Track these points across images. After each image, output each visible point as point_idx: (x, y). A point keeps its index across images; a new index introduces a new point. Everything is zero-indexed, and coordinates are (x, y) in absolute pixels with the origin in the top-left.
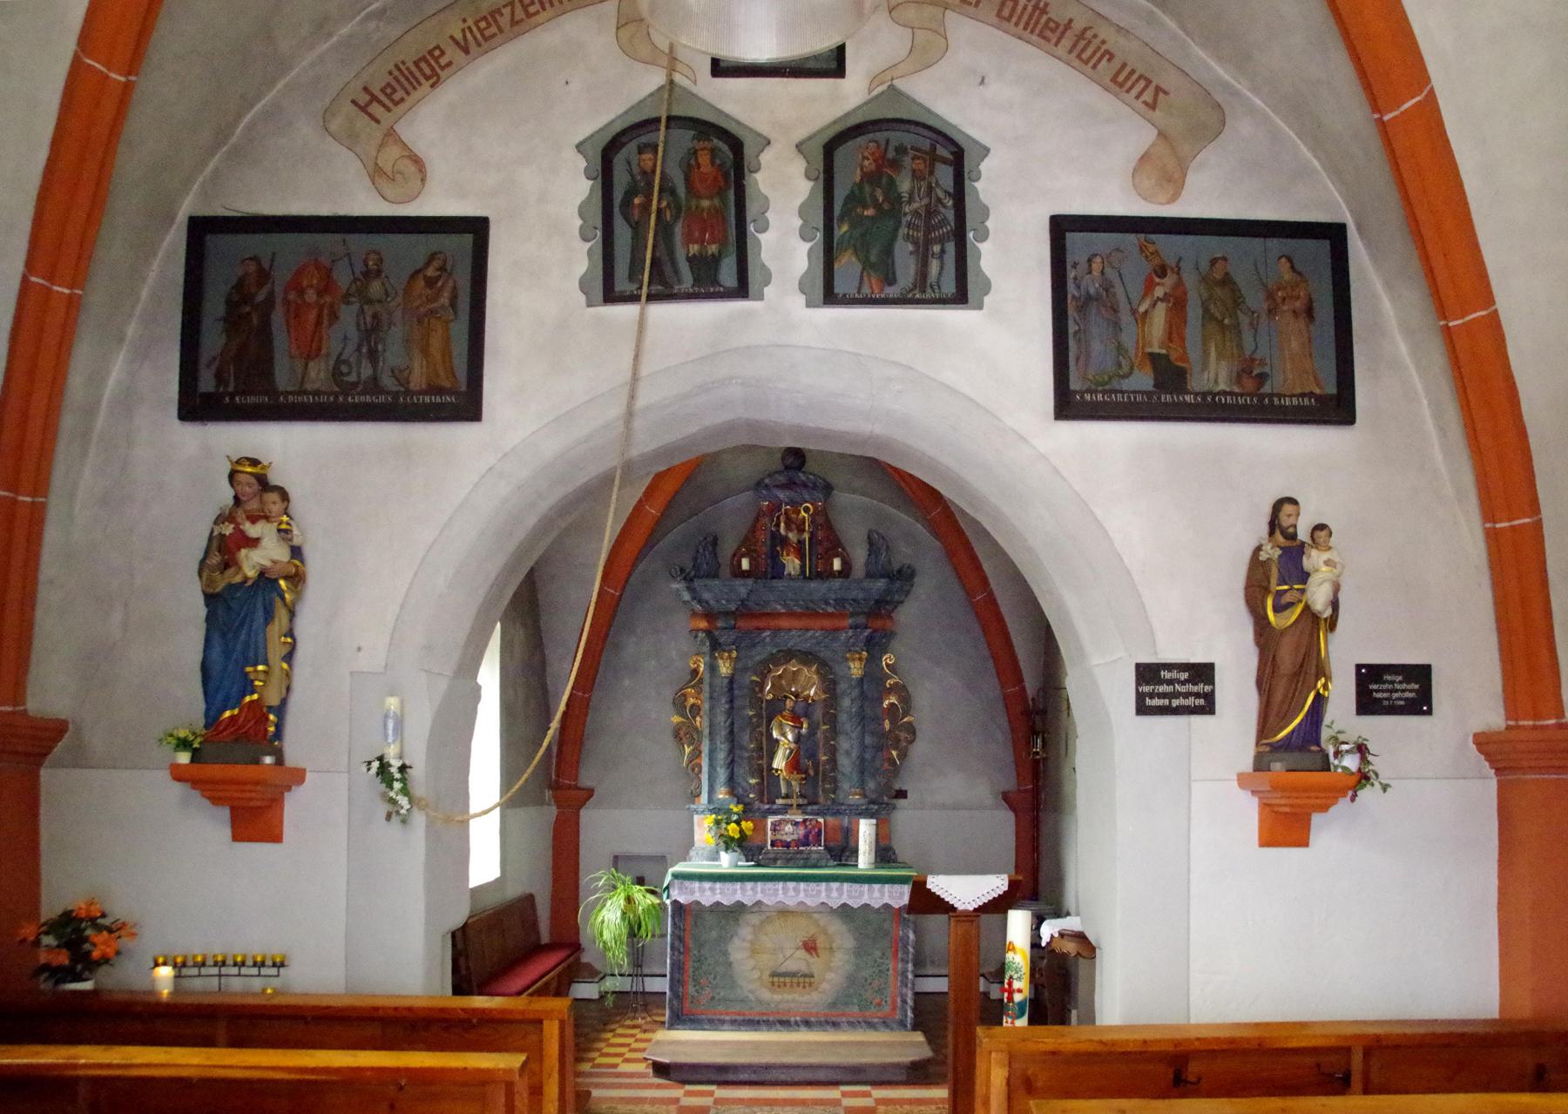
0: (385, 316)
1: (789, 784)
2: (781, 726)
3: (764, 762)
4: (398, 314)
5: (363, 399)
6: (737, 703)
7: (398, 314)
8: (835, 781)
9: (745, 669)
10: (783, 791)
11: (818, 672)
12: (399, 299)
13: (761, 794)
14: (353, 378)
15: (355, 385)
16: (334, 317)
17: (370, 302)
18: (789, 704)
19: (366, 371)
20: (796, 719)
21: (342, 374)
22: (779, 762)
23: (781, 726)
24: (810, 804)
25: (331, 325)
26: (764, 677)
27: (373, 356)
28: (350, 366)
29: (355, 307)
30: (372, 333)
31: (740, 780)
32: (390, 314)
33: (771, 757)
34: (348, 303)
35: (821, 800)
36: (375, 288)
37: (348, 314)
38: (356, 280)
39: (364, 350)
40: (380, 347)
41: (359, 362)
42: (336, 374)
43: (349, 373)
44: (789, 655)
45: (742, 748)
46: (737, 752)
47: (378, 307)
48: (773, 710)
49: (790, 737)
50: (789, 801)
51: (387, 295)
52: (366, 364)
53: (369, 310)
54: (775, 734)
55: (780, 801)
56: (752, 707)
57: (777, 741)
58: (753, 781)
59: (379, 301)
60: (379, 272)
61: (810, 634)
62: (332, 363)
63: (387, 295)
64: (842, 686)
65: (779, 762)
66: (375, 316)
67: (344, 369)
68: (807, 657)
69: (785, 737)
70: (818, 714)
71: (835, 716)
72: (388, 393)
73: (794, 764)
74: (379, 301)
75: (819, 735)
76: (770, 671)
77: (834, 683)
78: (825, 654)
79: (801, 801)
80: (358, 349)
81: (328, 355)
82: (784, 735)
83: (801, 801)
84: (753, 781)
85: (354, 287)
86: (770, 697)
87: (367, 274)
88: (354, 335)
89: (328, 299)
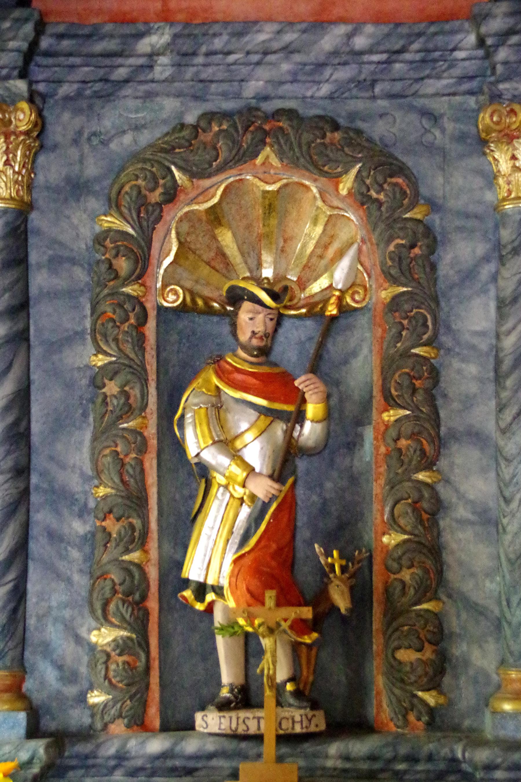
1: (250, 649)
2: (217, 408)
3: (150, 558)
6: (43, 318)
8: (437, 635)
9: (76, 188)
10: (228, 675)
11: (362, 198)
13: (135, 685)
18: (251, 322)
20: (278, 387)
22: (212, 555)
23: (217, 408)
24: (336, 729)
26: (148, 216)
31: (54, 633)
33: (181, 528)
35: (382, 705)
44: (251, 129)
45: (60, 497)
46: (41, 517)
48: (176, 351)
49: (256, 452)
50: (248, 721)
54: (196, 442)
55: (210, 721)
56: (99, 336)
57: (204, 471)
58: (104, 637)
61: (330, 40)
64: (461, 251)
65: (212, 555)
68: (318, 139)
69: (235, 455)
70: (364, 363)
71: (435, 374)
73: (275, 563)
75: (371, 446)
76: (172, 194)
77: (429, 239)
78: (390, 126)
79: (298, 718)
82: (227, 444)
83: (298, 718)
84: (104, 637)
86: (172, 300)
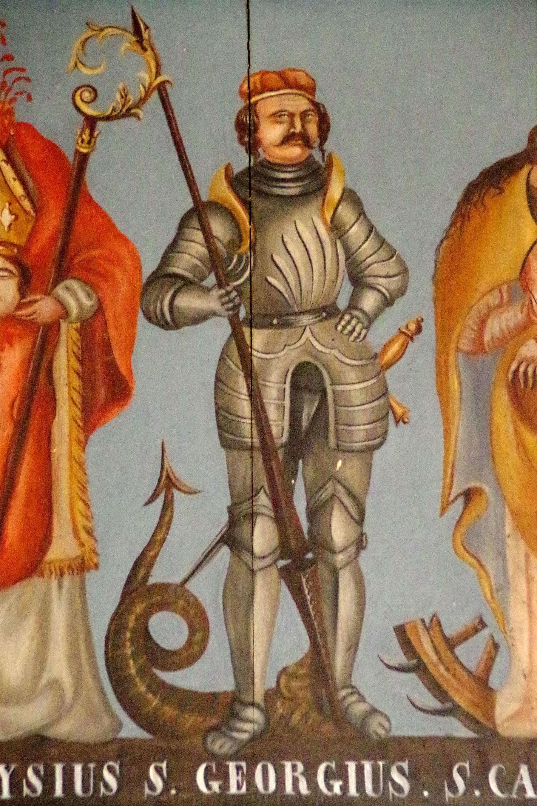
0: (353, 388)
4: (413, 380)
5: (265, 779)
7: (413, 380)
12: (419, 300)
14: (208, 675)
15: (224, 708)
16: (108, 388)
17: (278, 315)
19: (278, 638)
21: (155, 656)
25: (91, 416)
27: (304, 562)
28: (198, 623)
29: (219, 331)
30: (291, 458)
32: (377, 365)
34: (172, 322)
36: (300, 248)
37: (175, 369)
38: (199, 212)
39: (263, 536)
40: (339, 530)
41: (239, 601)
42: (129, 655)
43: (189, 655)
47: (312, 339)
51: (358, 281)
52: (269, 595)
53: (277, 355)
59: (327, 311)
60: (314, 177)
62: (105, 592)
63: (358, 281)
66: (306, 379)
67: (168, 630)
72: (390, 749)
74: (327, 311)
80: (232, 538)
81: (82, 567)
85: (195, 248)
87: (254, 182)
88: (210, 478)
89: (75, 297)
